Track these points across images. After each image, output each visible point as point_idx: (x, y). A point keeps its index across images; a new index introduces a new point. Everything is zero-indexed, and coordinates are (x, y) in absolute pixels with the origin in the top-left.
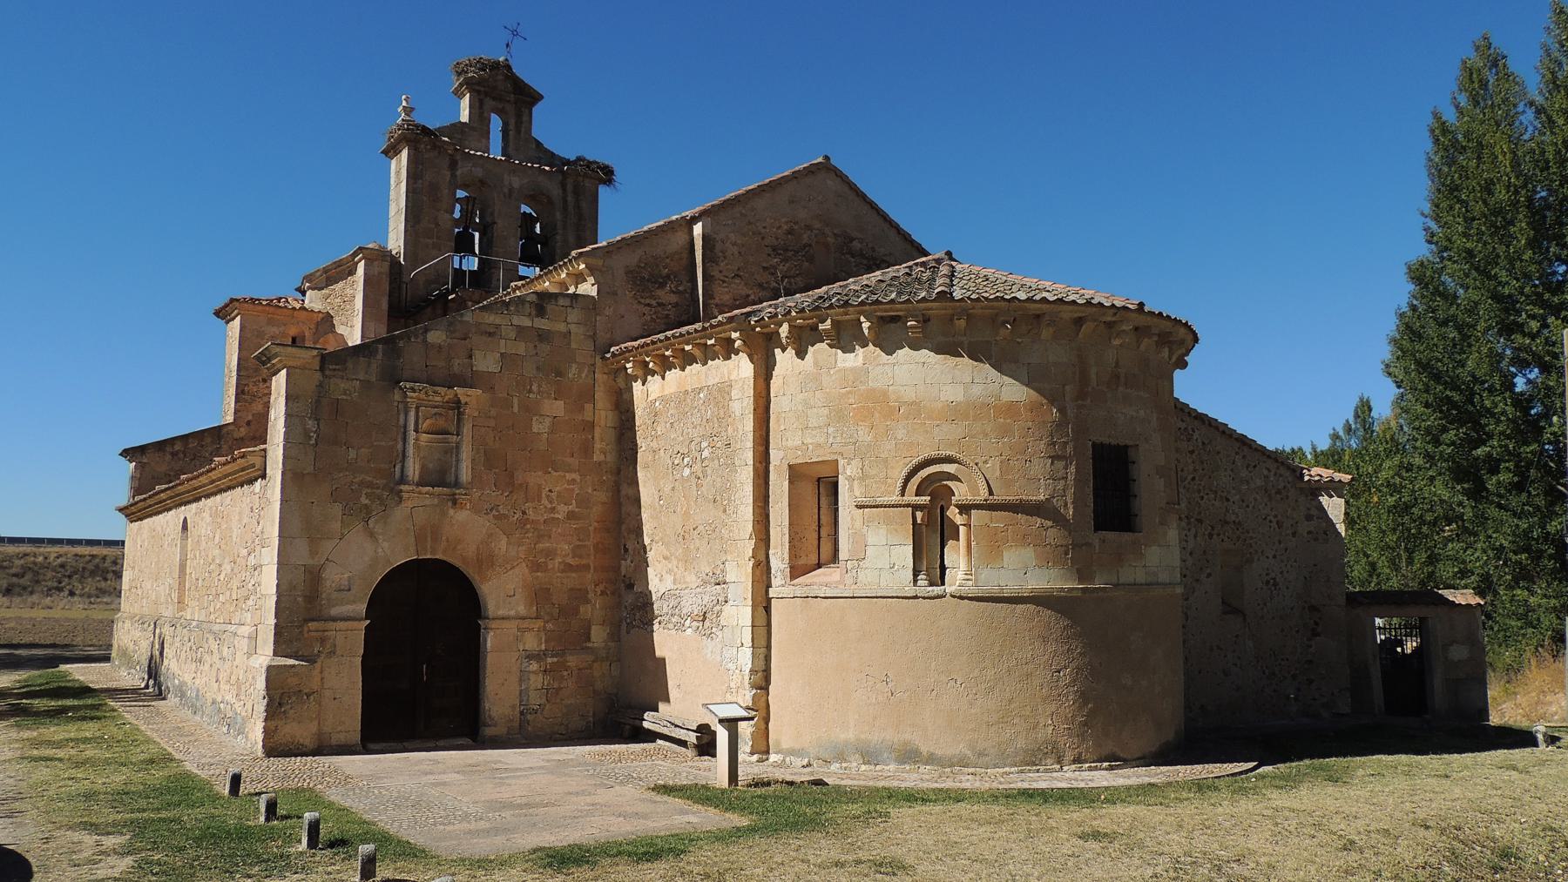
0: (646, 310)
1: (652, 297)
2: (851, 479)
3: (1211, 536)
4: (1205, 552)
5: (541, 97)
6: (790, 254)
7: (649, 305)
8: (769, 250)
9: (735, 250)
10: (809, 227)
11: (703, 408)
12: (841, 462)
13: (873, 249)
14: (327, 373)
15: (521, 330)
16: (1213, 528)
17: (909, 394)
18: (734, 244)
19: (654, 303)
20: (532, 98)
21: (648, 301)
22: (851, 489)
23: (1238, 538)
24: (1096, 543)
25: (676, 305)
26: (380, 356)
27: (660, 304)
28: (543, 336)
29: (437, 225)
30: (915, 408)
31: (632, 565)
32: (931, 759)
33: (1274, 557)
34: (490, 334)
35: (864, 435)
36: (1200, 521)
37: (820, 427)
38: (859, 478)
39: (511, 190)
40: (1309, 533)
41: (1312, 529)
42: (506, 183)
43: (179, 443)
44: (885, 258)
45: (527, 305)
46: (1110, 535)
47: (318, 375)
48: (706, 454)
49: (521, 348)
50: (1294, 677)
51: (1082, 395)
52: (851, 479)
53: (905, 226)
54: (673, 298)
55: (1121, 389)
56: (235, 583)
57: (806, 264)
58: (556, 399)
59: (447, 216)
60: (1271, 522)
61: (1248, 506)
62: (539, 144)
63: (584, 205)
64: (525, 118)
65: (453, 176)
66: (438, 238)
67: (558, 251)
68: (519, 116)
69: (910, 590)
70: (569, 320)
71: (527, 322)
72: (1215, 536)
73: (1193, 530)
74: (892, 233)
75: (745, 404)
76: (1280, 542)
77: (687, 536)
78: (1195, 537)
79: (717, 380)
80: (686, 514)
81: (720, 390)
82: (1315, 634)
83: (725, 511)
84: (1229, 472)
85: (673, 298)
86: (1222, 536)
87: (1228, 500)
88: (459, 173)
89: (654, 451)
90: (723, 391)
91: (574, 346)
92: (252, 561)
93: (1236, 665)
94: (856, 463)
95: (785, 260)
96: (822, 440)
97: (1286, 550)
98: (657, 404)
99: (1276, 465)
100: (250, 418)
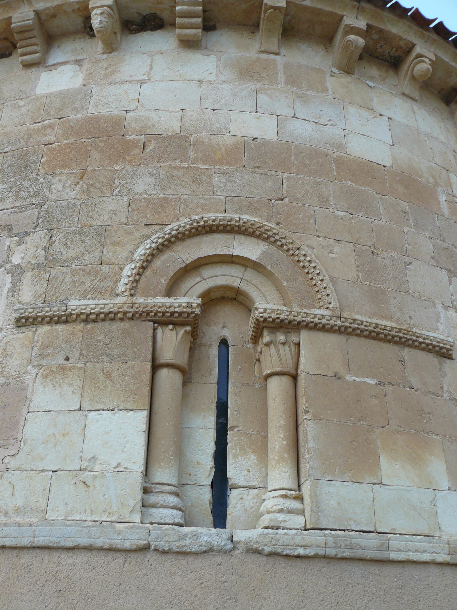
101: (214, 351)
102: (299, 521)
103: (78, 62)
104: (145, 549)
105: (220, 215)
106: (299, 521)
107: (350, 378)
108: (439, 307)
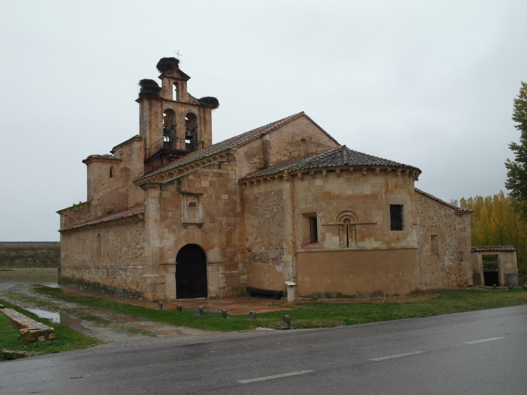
0: (250, 165)
2: (320, 217)
3: (428, 231)
4: (426, 235)
6: (293, 144)
7: (251, 163)
8: (286, 144)
9: (277, 145)
12: (318, 213)
13: (319, 141)
14: (162, 189)
15: (214, 173)
16: (428, 228)
17: (337, 193)
18: (276, 143)
19: (252, 162)
20: (188, 78)
21: (251, 162)
22: (320, 220)
23: (437, 231)
24: (392, 234)
25: (259, 163)
28: (220, 175)
29: (157, 127)
30: (339, 197)
31: (250, 244)
32: (346, 296)
33: (448, 236)
35: (324, 205)
36: (424, 226)
37: (310, 203)
38: (323, 217)
39: (181, 112)
40: (460, 229)
41: (460, 227)
43: (76, 207)
44: (323, 143)
45: (216, 165)
46: (395, 232)
47: (159, 191)
48: (275, 210)
49: (214, 179)
50: (455, 274)
51: (386, 192)
52: (320, 217)
53: (328, 132)
54: (258, 161)
55: (398, 189)
56: (130, 253)
57: (298, 147)
58: (225, 194)
59: (161, 123)
60: (447, 225)
61: (440, 221)
62: (190, 95)
63: (207, 116)
64: (184, 86)
65: (162, 109)
66: (158, 131)
68: (182, 85)
69: (338, 249)
70: (228, 170)
71: (216, 171)
72: (429, 231)
73: (422, 229)
74: (324, 136)
75: (288, 196)
76: (450, 232)
78: (423, 231)
79: (278, 189)
80: (269, 228)
81: (279, 191)
82: (462, 260)
83: (282, 227)
84: (433, 211)
85: (258, 161)
86: (431, 231)
87: (433, 219)
88: (164, 108)
89: (257, 210)
90: (280, 193)
92: (139, 246)
93: (436, 271)
94: (322, 212)
95: (292, 146)
96: (311, 206)
97: (452, 234)
98: (257, 195)
99: (449, 208)
100: (99, 198)
101: (346, 226)
102: (356, 246)
103: (321, 178)
104: (340, 251)
105: (345, 209)
106: (356, 246)
107: (362, 230)
108: (376, 216)
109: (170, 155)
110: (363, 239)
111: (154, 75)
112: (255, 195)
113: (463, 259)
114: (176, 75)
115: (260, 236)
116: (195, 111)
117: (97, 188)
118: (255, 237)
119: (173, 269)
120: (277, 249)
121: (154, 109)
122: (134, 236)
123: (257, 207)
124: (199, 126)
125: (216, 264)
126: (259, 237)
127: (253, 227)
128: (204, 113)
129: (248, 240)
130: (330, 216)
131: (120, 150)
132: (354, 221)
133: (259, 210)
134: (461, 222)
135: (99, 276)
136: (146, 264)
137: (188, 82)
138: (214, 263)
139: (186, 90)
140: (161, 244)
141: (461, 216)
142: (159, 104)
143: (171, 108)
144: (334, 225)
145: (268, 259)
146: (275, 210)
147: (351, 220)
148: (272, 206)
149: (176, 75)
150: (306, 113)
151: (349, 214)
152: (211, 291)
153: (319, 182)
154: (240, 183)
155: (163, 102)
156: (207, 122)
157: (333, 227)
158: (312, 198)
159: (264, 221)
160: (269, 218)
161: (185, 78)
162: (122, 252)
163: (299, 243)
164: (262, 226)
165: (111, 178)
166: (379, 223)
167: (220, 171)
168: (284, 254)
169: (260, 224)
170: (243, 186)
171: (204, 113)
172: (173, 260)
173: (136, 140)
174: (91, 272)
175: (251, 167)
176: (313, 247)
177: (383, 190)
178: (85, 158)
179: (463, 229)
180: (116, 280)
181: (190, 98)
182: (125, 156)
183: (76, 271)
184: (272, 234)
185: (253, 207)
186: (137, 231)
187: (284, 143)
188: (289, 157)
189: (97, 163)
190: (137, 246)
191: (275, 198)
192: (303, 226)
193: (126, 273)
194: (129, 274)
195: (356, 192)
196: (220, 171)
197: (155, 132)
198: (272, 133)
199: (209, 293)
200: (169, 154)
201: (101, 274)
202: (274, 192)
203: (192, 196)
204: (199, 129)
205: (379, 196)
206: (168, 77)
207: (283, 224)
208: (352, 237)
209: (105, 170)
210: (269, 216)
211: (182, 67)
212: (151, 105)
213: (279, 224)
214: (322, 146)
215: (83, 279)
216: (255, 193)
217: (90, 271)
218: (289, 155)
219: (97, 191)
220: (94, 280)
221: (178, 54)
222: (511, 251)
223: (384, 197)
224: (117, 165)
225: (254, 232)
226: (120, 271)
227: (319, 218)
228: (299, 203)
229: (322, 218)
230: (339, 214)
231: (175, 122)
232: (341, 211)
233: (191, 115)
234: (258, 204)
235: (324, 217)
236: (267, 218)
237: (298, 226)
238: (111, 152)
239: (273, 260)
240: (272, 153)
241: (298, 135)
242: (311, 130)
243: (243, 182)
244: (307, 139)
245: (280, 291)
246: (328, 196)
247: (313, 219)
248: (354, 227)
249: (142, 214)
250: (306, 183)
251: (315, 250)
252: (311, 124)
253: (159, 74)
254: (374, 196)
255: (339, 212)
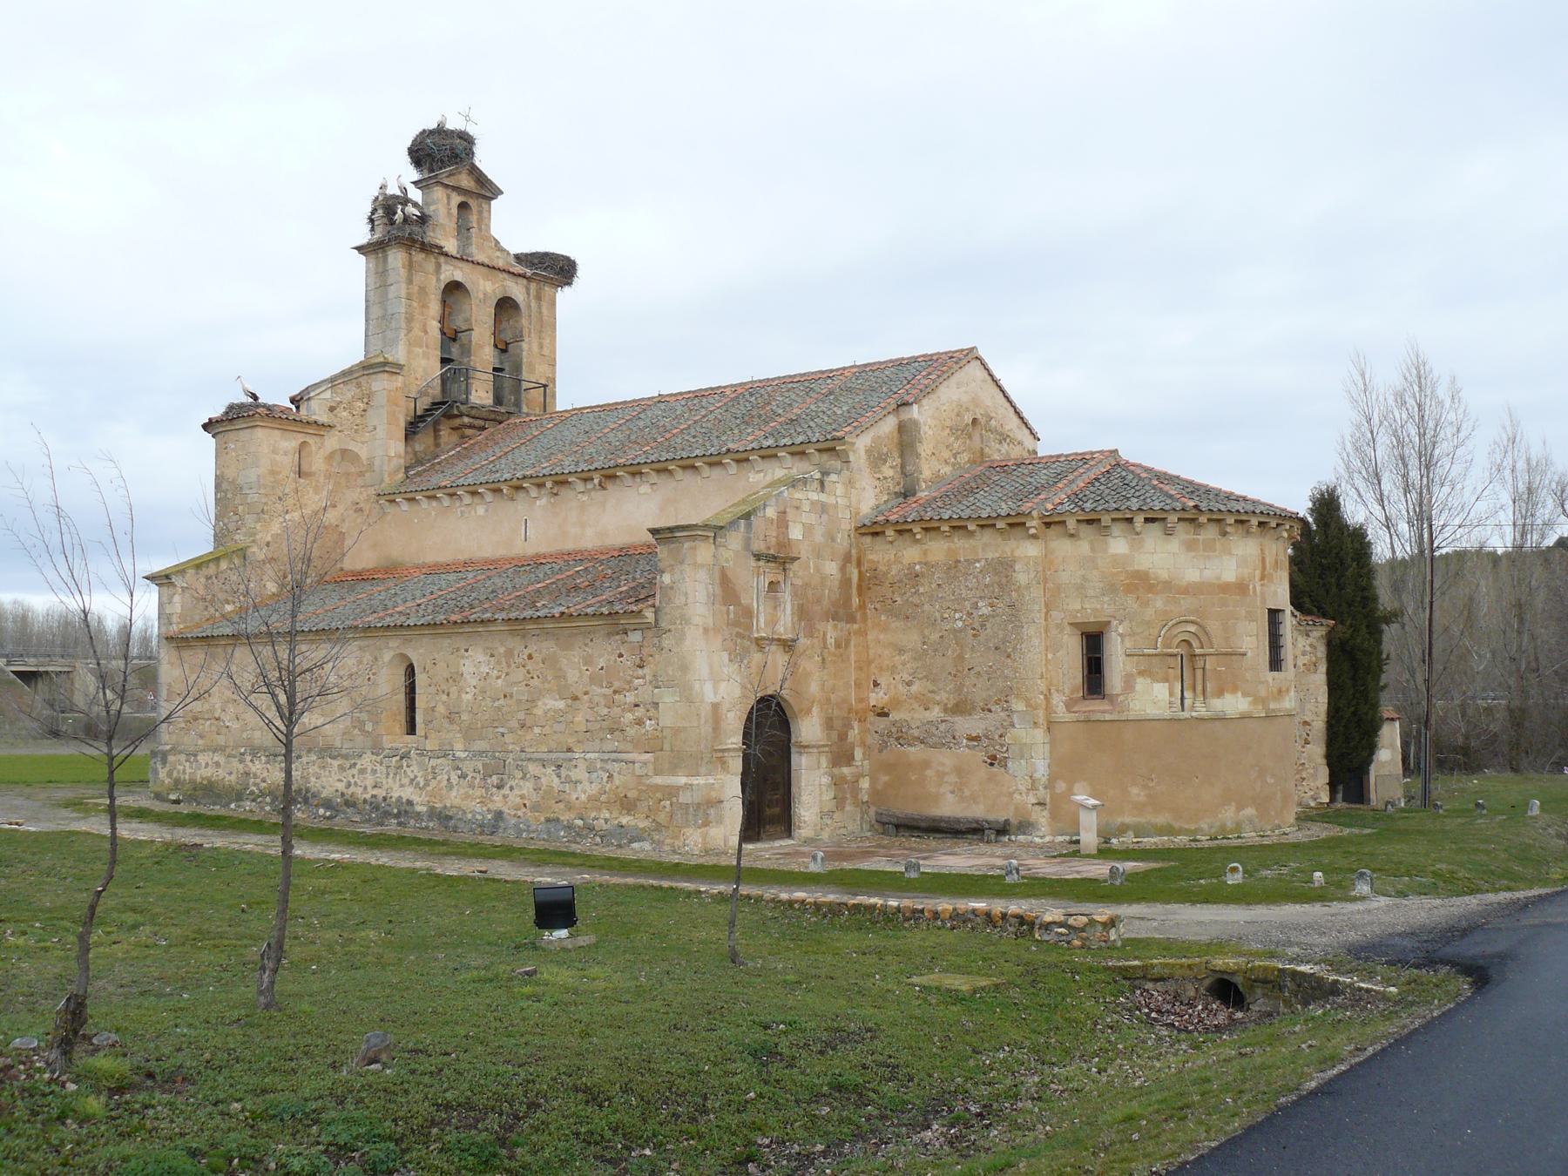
0: (877, 483)
1: (880, 472)
2: (1120, 635)
5: (502, 193)
8: (948, 431)
9: (930, 432)
10: (967, 410)
11: (980, 576)
12: (1115, 623)
15: (813, 503)
17: (1164, 575)
21: (878, 476)
22: (1122, 641)
24: (1270, 681)
25: (893, 478)
26: (742, 529)
27: (885, 478)
28: (823, 508)
29: (426, 332)
30: (1168, 586)
34: (797, 508)
35: (1131, 603)
37: (1097, 597)
40: (1304, 665)
42: (481, 288)
51: (1262, 579)
52: (1120, 635)
63: (545, 311)
64: (485, 214)
65: (438, 280)
66: (427, 347)
67: (525, 360)
68: (480, 212)
69: (1167, 714)
71: (814, 496)
77: (959, 674)
79: (997, 555)
83: (1009, 656)
88: (442, 277)
90: (1004, 567)
91: (840, 516)
94: (1126, 623)
95: (957, 439)
96: (1099, 606)
98: (918, 567)
100: (269, 539)
103: (1125, 537)
109: (466, 420)
110: (1220, 693)
111: (402, 175)
112: (911, 566)
113: (1310, 739)
114: (465, 181)
115: (926, 677)
116: (517, 291)
117: (265, 508)
118: (907, 678)
119: (737, 764)
120: (990, 711)
121: (418, 278)
122: (602, 669)
123: (916, 600)
124: (526, 339)
125: (815, 750)
126: (920, 679)
127: (901, 651)
128: (539, 298)
129: (876, 684)
130: (1146, 633)
131: (328, 395)
132: (1202, 648)
133: (926, 607)
134: (1308, 648)
135: (406, 781)
136: (667, 747)
137: (493, 202)
138: (813, 747)
139: (488, 226)
140: (716, 693)
141: (1308, 635)
142: (430, 264)
143: (459, 279)
144: (1156, 655)
145: (954, 738)
146: (985, 610)
147: (1194, 645)
148: (976, 600)
149: (465, 181)
150: (982, 353)
151: (1192, 628)
152: (805, 822)
153: (1118, 545)
154: (863, 531)
155: (442, 259)
156: (547, 326)
157: (1154, 660)
158: (1101, 585)
159: (941, 637)
160: (960, 630)
161: (486, 190)
162: (539, 712)
163: (1058, 701)
164: (936, 650)
165: (302, 481)
166: (1249, 654)
167: (823, 497)
168: (1013, 725)
169: (924, 643)
170: (868, 539)
171: (539, 298)
172: (735, 740)
173: (387, 369)
174: (358, 767)
175: (878, 490)
176: (1096, 706)
177: (1258, 573)
178: (217, 412)
179: (1312, 667)
180: (506, 791)
181: (498, 254)
182: (345, 414)
183: (267, 763)
184: (972, 672)
185: (898, 599)
186: (621, 656)
187: (943, 429)
188: (953, 465)
189: (267, 431)
190: (616, 697)
191: (984, 578)
192: (1072, 654)
193: (563, 772)
194: (579, 773)
195: (1208, 574)
196: (823, 497)
197: (421, 347)
198: (925, 402)
199: (799, 828)
200: (461, 415)
201: (419, 775)
202: (983, 562)
203: (773, 565)
204: (525, 345)
205: (1251, 587)
206: (447, 186)
207: (1015, 649)
208: (1194, 689)
209: (286, 453)
210: (960, 624)
211: (484, 159)
212: (410, 266)
213: (996, 648)
214: (1008, 440)
215: (308, 790)
216: (906, 561)
217: (355, 764)
218: (953, 460)
219: (266, 516)
220: (380, 793)
221: (467, 119)
222: (1393, 719)
223: (1258, 589)
224: (317, 439)
225: (904, 664)
226: (533, 768)
227: (1119, 638)
228: (1063, 595)
229: (1127, 639)
230: (1170, 629)
231: (467, 320)
232: (1174, 621)
233: (505, 305)
234: (921, 590)
235: (1132, 634)
236: (955, 631)
237: (1058, 654)
238: (293, 400)
239: (971, 739)
240: (923, 453)
241: (967, 410)
242: (990, 397)
243: (872, 530)
244: (983, 421)
245: (1006, 820)
246: (1141, 583)
247: (1093, 643)
248: (1202, 662)
249: (653, 610)
250: (1084, 547)
251: (1108, 717)
252: (989, 378)
253: (415, 175)
254: (1241, 588)
255: (1170, 624)
